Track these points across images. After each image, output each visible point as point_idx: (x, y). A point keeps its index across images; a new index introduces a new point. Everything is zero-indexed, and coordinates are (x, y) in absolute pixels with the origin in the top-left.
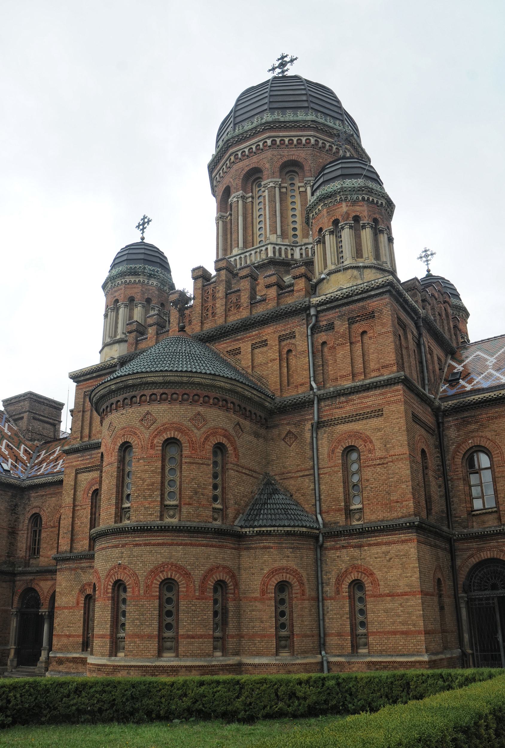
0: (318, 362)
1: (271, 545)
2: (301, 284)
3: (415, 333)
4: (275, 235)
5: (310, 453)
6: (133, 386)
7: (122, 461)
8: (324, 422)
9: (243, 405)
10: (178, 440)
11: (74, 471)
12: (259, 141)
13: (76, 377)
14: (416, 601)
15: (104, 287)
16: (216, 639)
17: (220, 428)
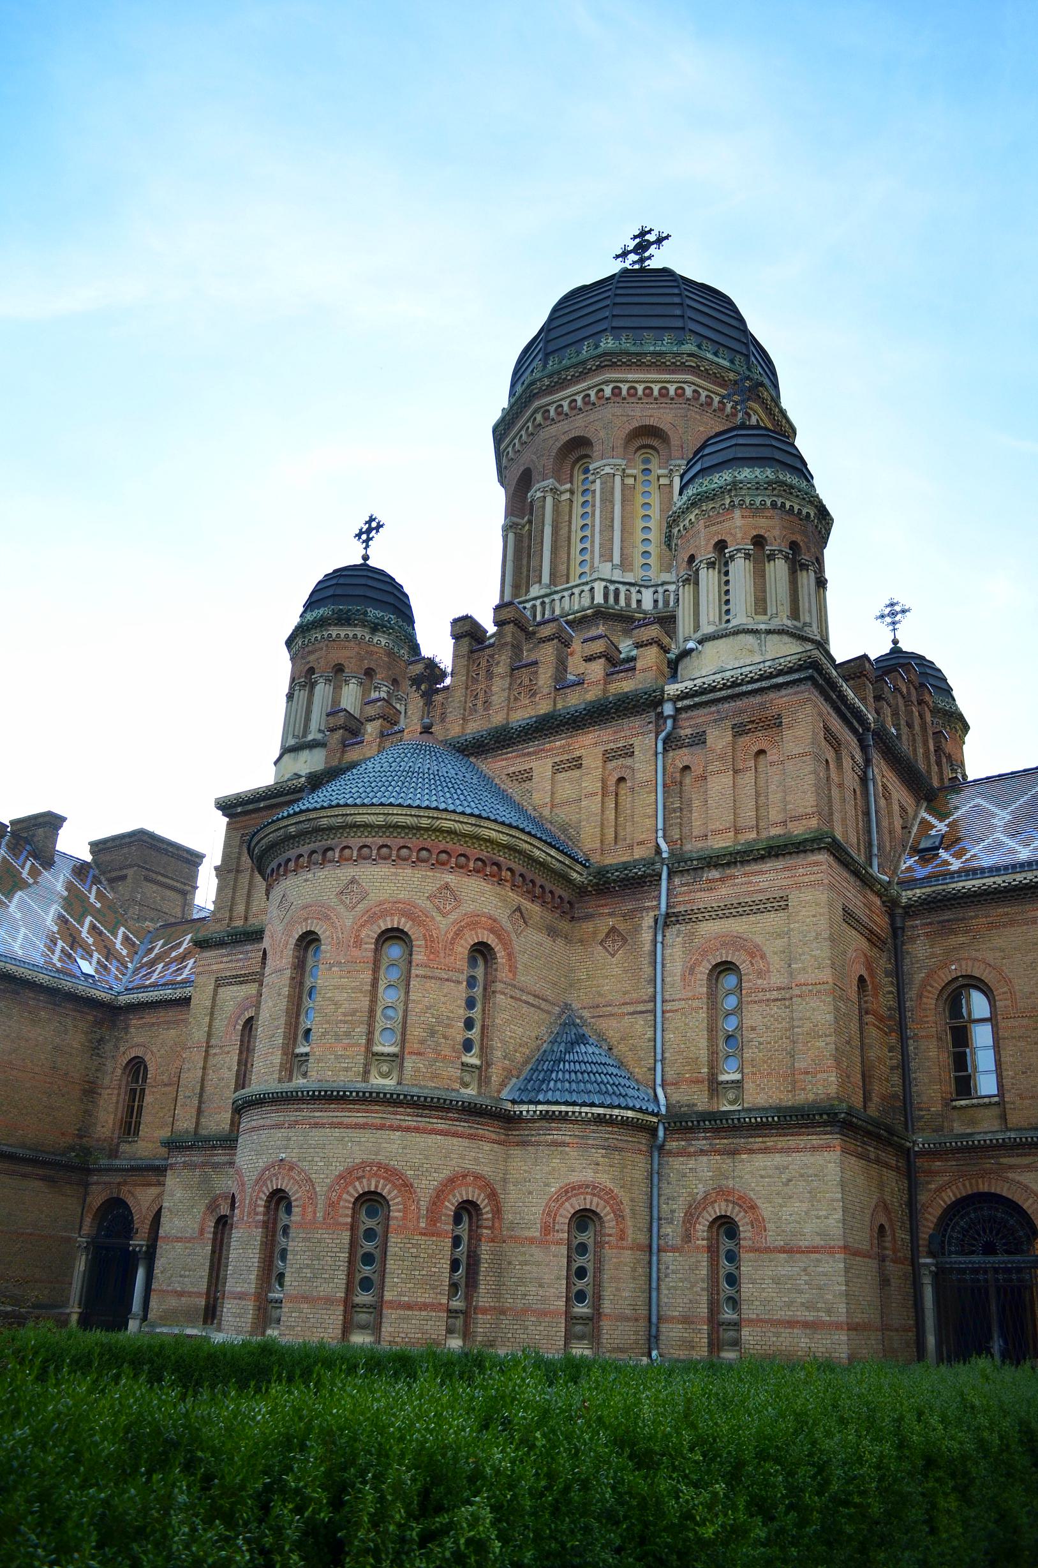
0: (672, 803)
1: (567, 1139)
2: (649, 658)
3: (859, 757)
4: (609, 565)
5: (648, 970)
6: (330, 828)
7: (300, 966)
8: (676, 915)
9: (530, 876)
10: (406, 934)
11: (213, 981)
12: (589, 389)
13: (229, 807)
14: (833, 1267)
15: (289, 643)
16: (452, 1313)
17: (484, 915)
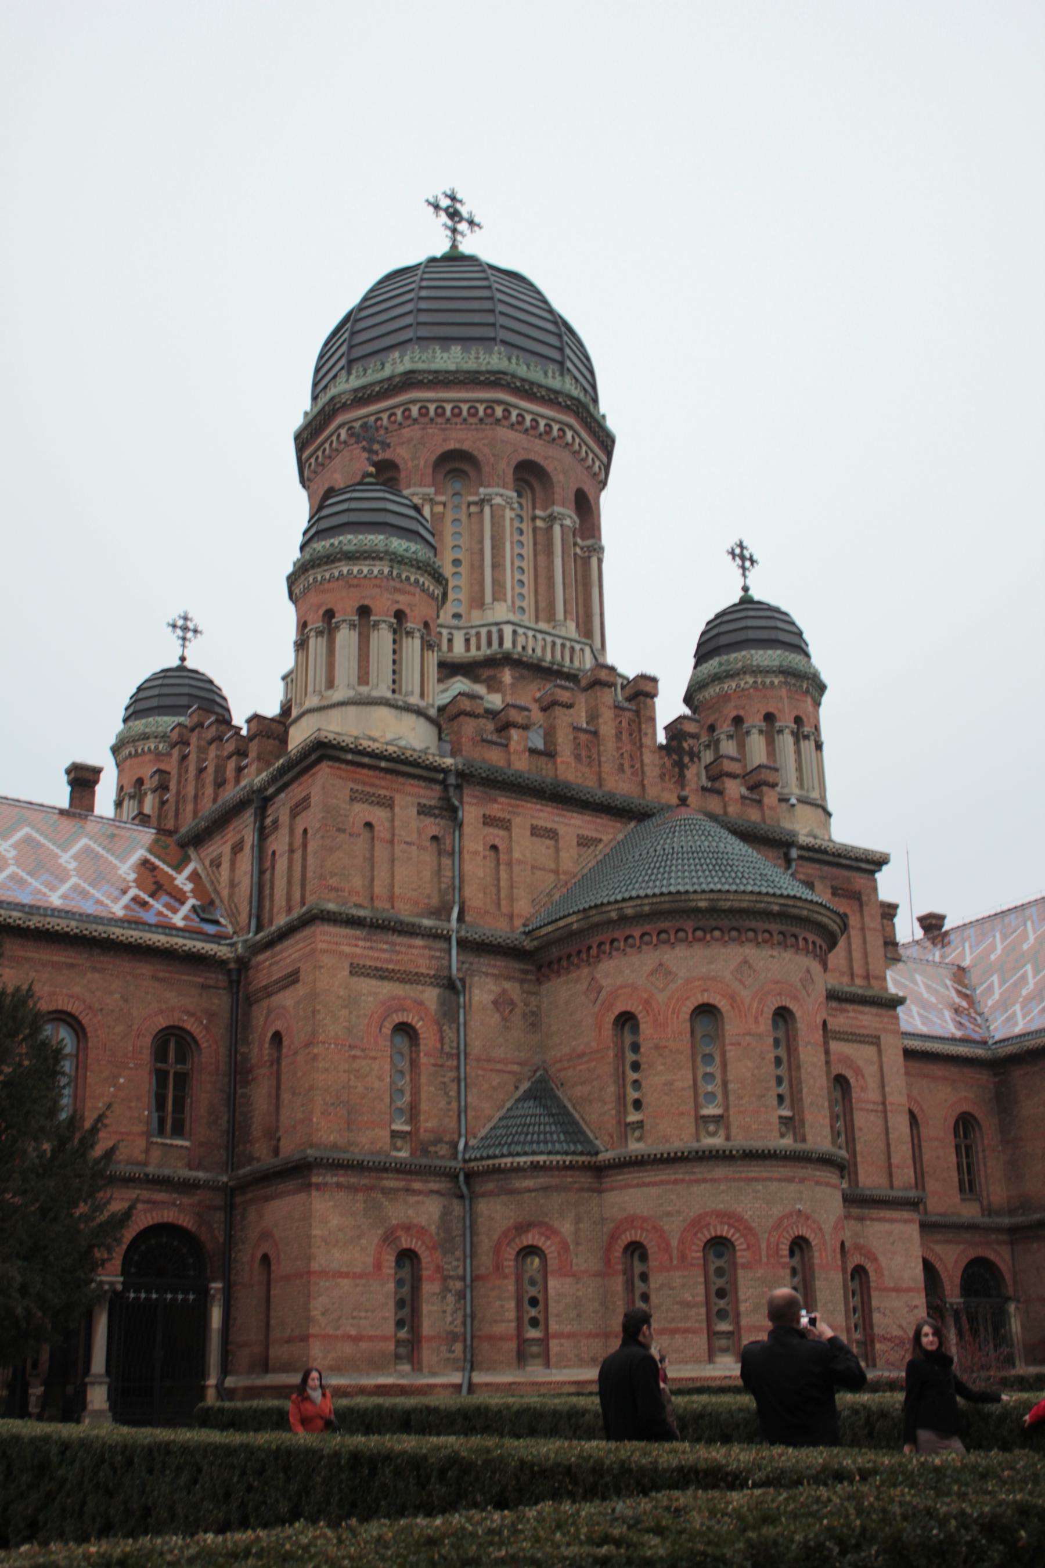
11: (347, 966)
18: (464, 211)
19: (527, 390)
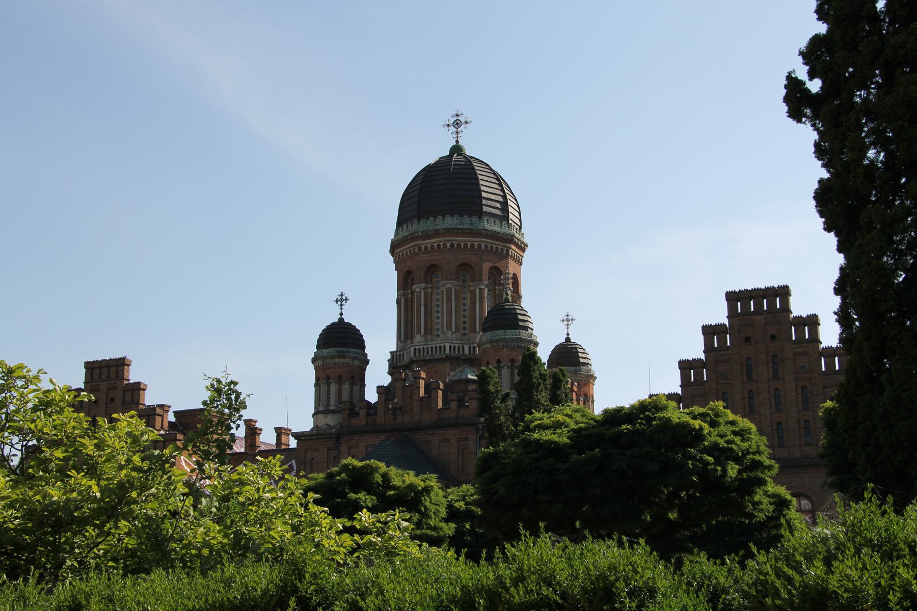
18: (462, 119)
19: (426, 236)
